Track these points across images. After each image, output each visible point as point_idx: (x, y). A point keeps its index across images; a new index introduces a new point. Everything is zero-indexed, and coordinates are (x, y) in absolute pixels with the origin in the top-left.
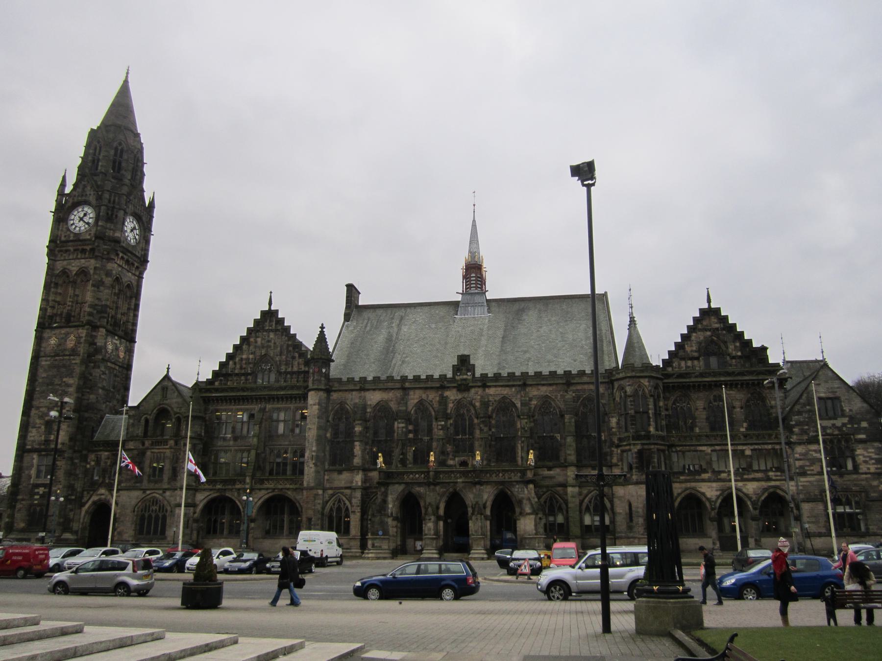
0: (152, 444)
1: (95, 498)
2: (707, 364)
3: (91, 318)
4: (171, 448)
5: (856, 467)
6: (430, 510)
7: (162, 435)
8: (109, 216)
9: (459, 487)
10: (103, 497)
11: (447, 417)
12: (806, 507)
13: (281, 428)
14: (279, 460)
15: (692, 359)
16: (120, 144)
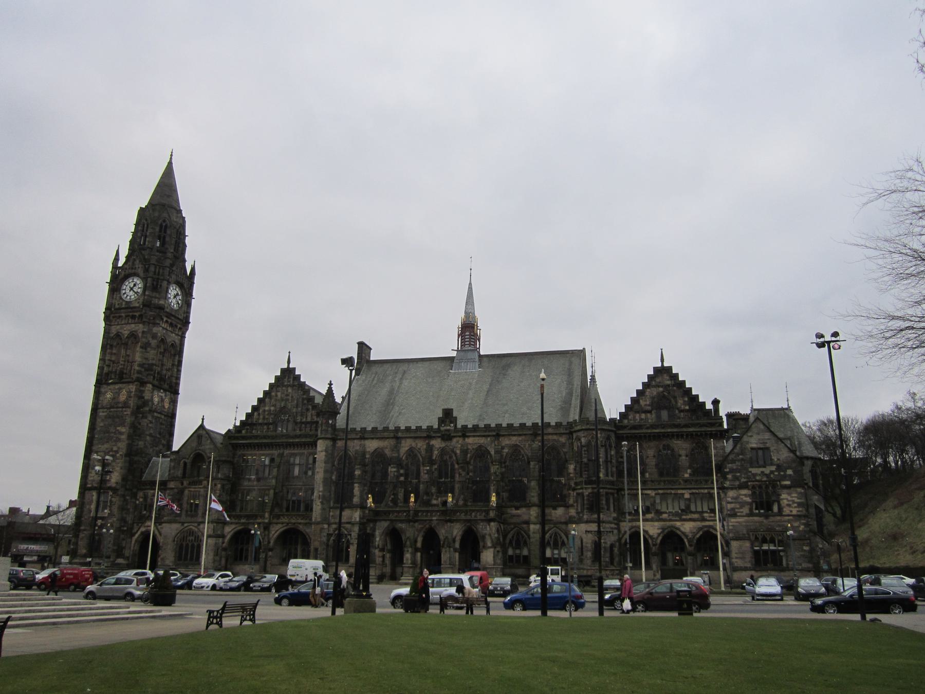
0: (189, 484)
2: (659, 417)
3: (140, 376)
5: (780, 509)
6: (408, 543)
7: (198, 476)
8: (155, 286)
9: (434, 523)
11: (431, 462)
13: (296, 471)
14: (294, 498)
15: (646, 412)
16: (164, 221)
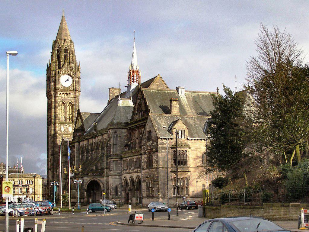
12: (143, 183)
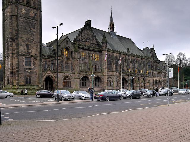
1: (47, 75)
4: (71, 61)
10: (50, 74)
